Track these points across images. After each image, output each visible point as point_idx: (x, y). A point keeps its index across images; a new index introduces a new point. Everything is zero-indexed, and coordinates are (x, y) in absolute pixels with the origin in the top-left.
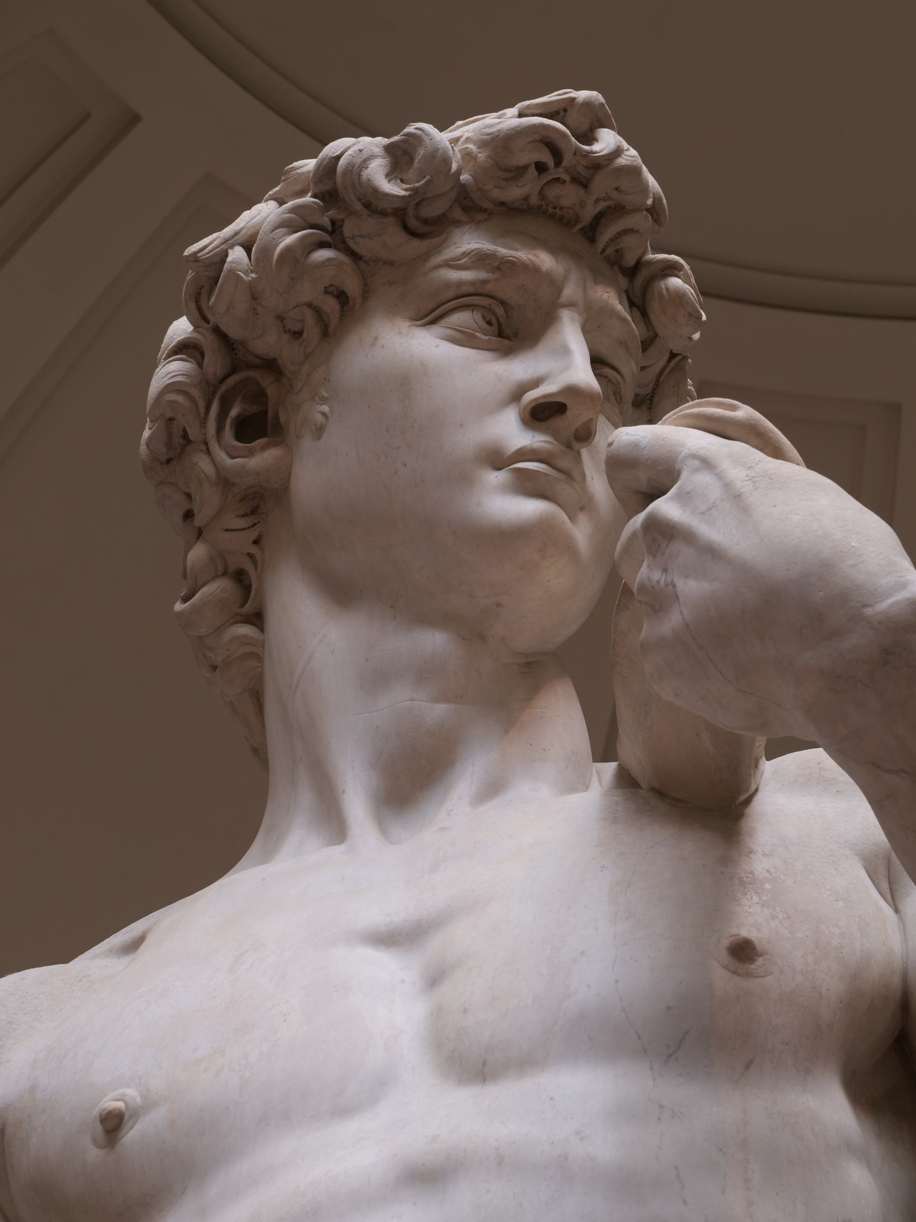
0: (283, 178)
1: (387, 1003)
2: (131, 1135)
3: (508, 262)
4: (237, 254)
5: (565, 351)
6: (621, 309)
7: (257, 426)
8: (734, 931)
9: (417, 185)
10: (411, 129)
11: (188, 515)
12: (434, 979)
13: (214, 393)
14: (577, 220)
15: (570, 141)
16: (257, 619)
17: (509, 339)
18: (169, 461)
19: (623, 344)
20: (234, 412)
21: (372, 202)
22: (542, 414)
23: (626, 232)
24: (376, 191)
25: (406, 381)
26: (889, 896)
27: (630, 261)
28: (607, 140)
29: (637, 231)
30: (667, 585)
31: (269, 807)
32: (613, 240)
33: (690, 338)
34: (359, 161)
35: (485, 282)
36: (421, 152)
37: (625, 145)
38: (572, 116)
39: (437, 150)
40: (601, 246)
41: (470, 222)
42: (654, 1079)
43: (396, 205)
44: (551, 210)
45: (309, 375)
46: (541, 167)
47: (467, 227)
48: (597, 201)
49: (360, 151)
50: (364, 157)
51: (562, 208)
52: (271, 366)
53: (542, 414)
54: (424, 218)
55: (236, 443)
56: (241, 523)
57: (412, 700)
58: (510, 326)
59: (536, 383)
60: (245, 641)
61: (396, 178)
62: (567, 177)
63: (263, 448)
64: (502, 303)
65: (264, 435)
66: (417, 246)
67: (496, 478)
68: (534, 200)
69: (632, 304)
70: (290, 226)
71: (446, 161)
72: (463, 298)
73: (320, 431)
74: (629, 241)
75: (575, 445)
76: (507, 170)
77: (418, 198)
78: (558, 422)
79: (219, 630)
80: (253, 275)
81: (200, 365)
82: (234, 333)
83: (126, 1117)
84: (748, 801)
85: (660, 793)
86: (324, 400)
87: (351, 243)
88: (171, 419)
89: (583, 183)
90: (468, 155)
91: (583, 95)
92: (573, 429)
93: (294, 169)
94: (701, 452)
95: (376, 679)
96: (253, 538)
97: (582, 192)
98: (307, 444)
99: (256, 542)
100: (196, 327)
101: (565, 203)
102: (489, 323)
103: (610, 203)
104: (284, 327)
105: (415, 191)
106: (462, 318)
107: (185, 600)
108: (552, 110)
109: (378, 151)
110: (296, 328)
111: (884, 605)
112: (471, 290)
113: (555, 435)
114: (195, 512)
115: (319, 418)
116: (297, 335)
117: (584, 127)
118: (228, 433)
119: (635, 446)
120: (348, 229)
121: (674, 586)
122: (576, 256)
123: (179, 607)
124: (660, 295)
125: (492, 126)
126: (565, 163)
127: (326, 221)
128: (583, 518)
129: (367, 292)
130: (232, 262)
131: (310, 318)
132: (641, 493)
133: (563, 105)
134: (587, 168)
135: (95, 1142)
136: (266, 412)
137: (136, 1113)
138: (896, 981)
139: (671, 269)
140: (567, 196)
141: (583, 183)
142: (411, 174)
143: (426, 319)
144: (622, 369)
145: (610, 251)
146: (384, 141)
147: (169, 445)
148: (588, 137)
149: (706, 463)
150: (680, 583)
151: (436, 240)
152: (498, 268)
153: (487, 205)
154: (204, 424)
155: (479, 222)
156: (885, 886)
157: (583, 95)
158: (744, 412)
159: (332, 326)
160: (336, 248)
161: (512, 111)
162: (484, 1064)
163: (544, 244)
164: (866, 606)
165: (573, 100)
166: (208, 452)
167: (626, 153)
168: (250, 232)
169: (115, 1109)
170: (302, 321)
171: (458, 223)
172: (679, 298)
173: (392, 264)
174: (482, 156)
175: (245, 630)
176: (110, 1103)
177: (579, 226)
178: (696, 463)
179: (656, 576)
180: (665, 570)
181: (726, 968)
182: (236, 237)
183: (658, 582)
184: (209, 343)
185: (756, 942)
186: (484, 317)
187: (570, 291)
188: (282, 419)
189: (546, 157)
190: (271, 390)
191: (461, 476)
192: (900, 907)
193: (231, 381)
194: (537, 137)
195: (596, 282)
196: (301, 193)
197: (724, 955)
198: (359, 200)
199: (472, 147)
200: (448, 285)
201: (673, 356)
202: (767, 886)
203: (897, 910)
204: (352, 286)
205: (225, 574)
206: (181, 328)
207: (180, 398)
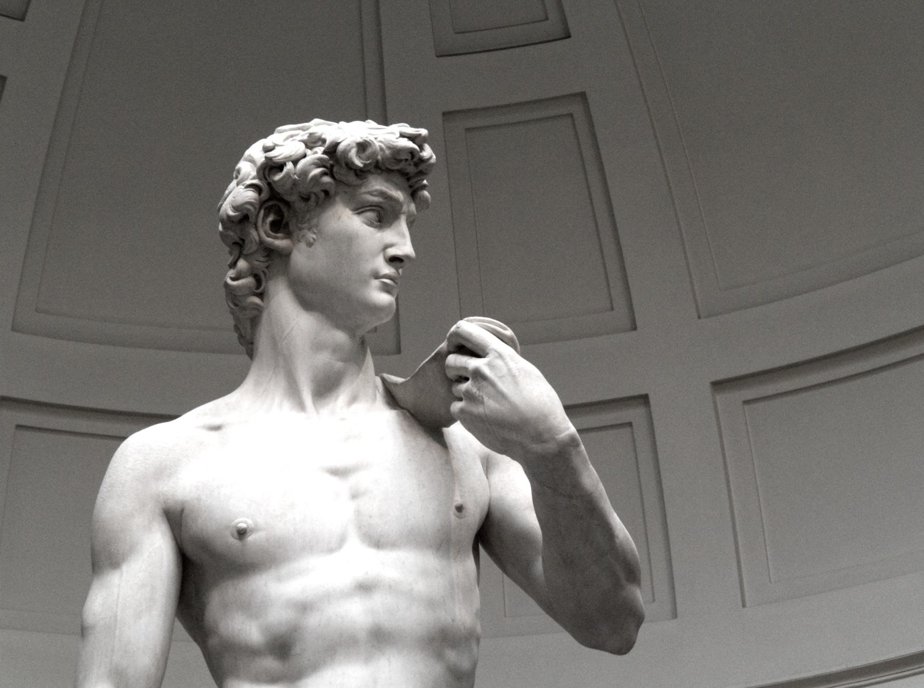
2: (251, 538)
5: (403, 236)
7: (278, 226)
12: (354, 496)
21: (350, 166)
24: (353, 163)
25: (349, 239)
36: (369, 151)
38: (417, 140)
46: (406, 160)
47: (375, 176)
52: (288, 204)
53: (394, 260)
56: (262, 259)
58: (383, 215)
63: (282, 239)
66: (359, 182)
67: (376, 283)
70: (318, 166)
72: (372, 207)
73: (310, 245)
77: (365, 165)
78: (398, 264)
81: (260, 194)
85: (412, 415)
90: (381, 149)
94: (499, 350)
95: (318, 347)
98: (303, 245)
99: (267, 268)
106: (371, 215)
107: (233, 279)
109: (354, 145)
115: (312, 240)
118: (267, 227)
119: (471, 335)
120: (335, 169)
127: (329, 165)
129: (336, 194)
135: (233, 536)
140: (411, 169)
142: (363, 155)
148: (422, 148)
149: (500, 356)
150: (486, 399)
154: (257, 216)
158: (509, 332)
165: (420, 135)
166: (256, 229)
171: (372, 173)
172: (425, 200)
173: (348, 185)
174: (387, 152)
175: (257, 300)
179: (474, 390)
180: (479, 389)
187: (405, 208)
189: (409, 157)
190: (286, 214)
191: (365, 282)
193: (270, 203)
197: (453, 509)
200: (368, 202)
204: (332, 192)
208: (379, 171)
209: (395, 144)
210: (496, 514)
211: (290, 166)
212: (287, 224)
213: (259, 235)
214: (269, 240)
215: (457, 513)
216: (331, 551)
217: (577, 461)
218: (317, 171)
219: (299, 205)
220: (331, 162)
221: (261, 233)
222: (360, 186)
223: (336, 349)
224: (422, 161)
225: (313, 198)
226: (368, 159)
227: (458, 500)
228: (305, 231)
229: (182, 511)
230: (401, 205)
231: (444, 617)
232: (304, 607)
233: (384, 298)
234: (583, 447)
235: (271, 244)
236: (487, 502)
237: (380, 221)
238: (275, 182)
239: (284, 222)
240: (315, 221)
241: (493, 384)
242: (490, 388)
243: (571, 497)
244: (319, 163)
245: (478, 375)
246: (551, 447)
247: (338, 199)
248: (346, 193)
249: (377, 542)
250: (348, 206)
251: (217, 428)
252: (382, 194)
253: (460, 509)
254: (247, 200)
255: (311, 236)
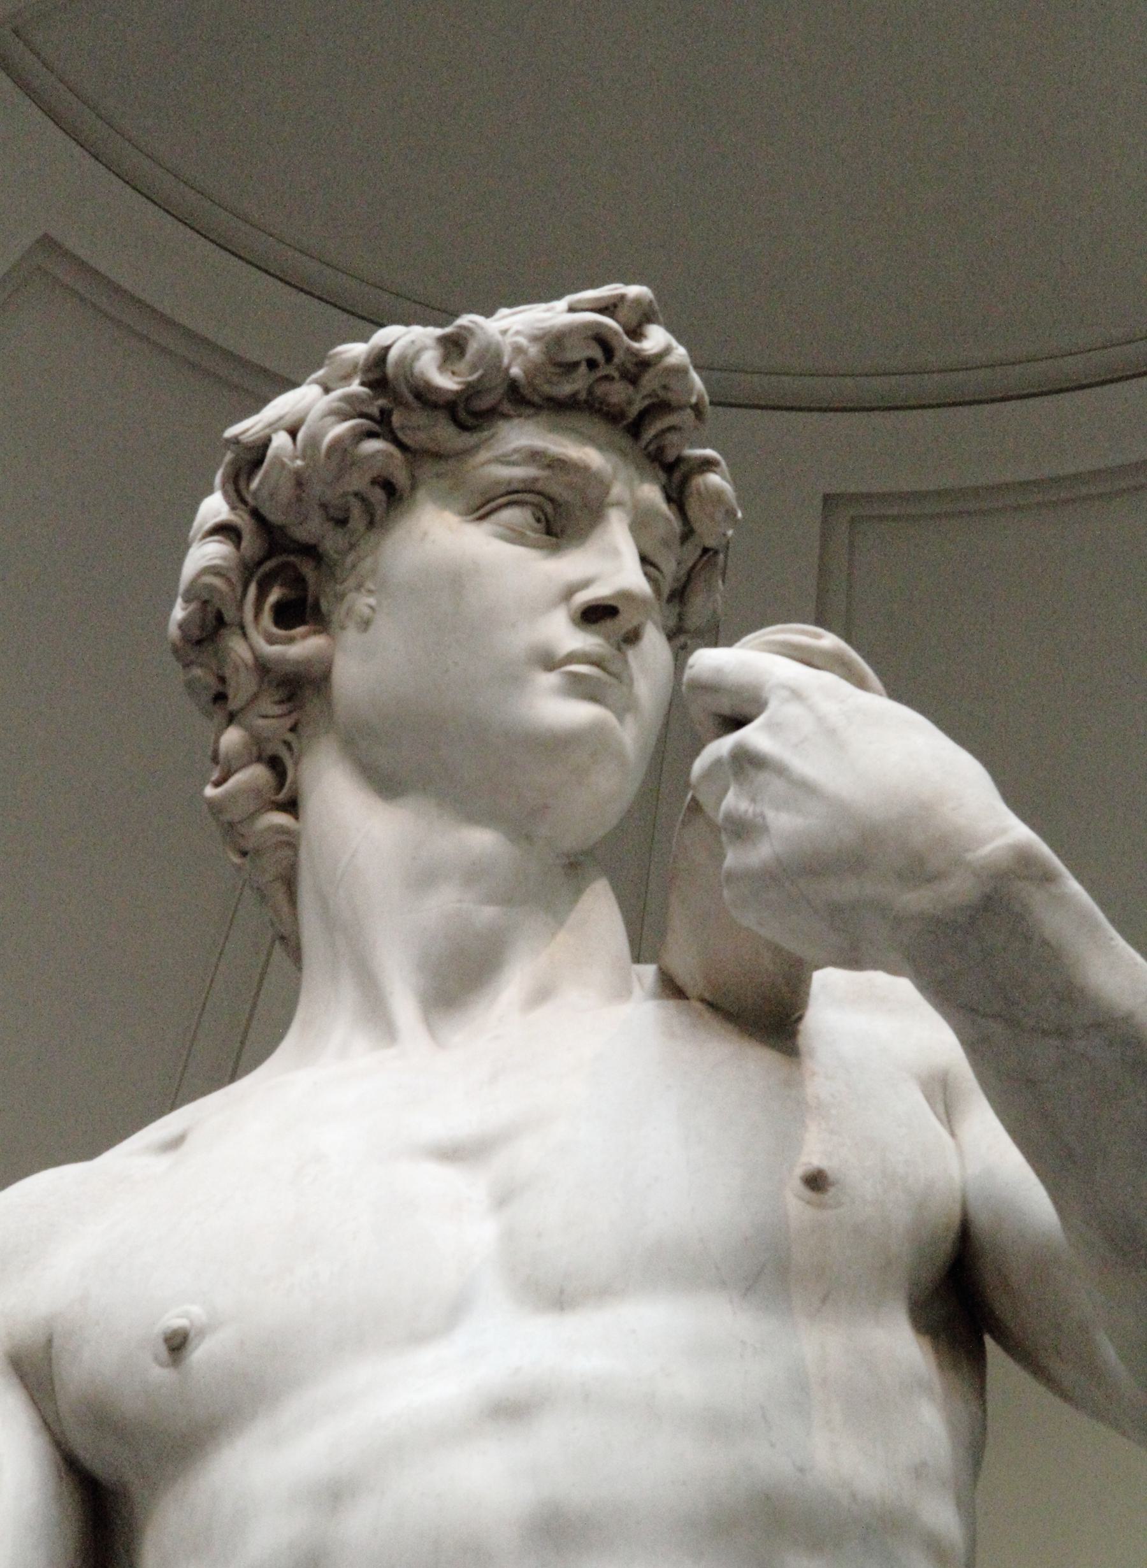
0: (327, 362)
1: (460, 1226)
2: (199, 1354)
3: (559, 460)
4: (281, 440)
5: (616, 553)
6: (664, 507)
7: (297, 612)
8: (804, 1159)
9: (470, 379)
10: (465, 320)
11: (220, 698)
12: (503, 1199)
13: (252, 575)
14: (622, 415)
15: (622, 340)
16: (291, 806)
17: (556, 536)
18: (199, 642)
19: (665, 543)
20: (274, 596)
21: (425, 397)
22: (594, 615)
23: (671, 429)
25: (456, 579)
26: (944, 1117)
27: (671, 456)
28: (656, 338)
29: (680, 429)
30: (755, 815)
31: (303, 999)
32: (656, 437)
33: (725, 535)
34: (411, 352)
35: (536, 480)
36: (473, 347)
37: (674, 343)
38: (623, 312)
39: (489, 344)
40: (643, 443)
41: (520, 416)
42: (735, 1313)
43: (451, 397)
44: (597, 405)
45: (354, 566)
46: (592, 364)
47: (516, 421)
48: (644, 398)
49: (413, 342)
50: (416, 348)
51: (608, 405)
52: (311, 551)
53: (594, 615)
54: (471, 412)
55: (275, 630)
56: (277, 710)
57: (460, 901)
59: (586, 584)
60: (281, 830)
61: (447, 369)
62: (616, 375)
63: (304, 637)
64: (552, 500)
65: (303, 622)
68: (583, 396)
69: (669, 499)
71: (498, 355)
73: (365, 624)
74: (672, 437)
75: (624, 646)
76: (559, 365)
77: (471, 391)
78: (609, 624)
79: (253, 816)
80: (299, 463)
82: (275, 517)
83: (192, 1334)
84: (800, 1018)
85: (713, 1006)
86: (370, 592)
87: (400, 435)
88: (205, 603)
89: (633, 380)
90: (518, 350)
91: (634, 291)
92: (624, 631)
93: (340, 353)
95: (424, 878)
96: (288, 726)
97: (631, 388)
98: (351, 636)
99: (293, 729)
100: (233, 508)
101: (614, 399)
102: (538, 520)
103: (655, 400)
104: (327, 513)
105: (469, 385)
107: (217, 784)
108: (603, 304)
109: (430, 342)
110: (340, 515)
111: (986, 850)
112: (521, 486)
113: (607, 638)
114: (231, 697)
115: (367, 611)
116: (342, 522)
117: (634, 323)
119: (719, 671)
120: (396, 419)
121: (764, 818)
122: (623, 453)
123: (210, 791)
124: (699, 494)
125: (543, 320)
126: (616, 360)
127: (374, 410)
128: (629, 719)
130: (277, 448)
131: (356, 511)
132: (720, 716)
133: (612, 301)
134: (636, 364)
135: (156, 1358)
136: (306, 596)
137: (202, 1333)
138: (957, 1209)
139: (708, 465)
140: (617, 392)
141: (633, 380)
142: (462, 366)
143: (477, 514)
144: (663, 567)
145: (652, 448)
146: (439, 332)
147: (202, 628)
148: (636, 333)
149: (796, 694)
151: (486, 434)
152: (549, 466)
153: (536, 399)
154: (240, 606)
155: (528, 417)
156: (941, 1109)
157: (634, 291)
158: (829, 641)
159: (378, 518)
160: (386, 439)
161: (562, 304)
162: (562, 1292)
163: (591, 440)
164: (967, 850)
165: (622, 297)
166: (245, 635)
167: (675, 351)
168: (295, 418)
169: (180, 1328)
170: (348, 510)
171: (506, 417)
172: (717, 497)
173: (438, 456)
174: (533, 350)
175: (280, 819)
176: (174, 1320)
177: (625, 423)
178: (785, 693)
180: (753, 800)
181: (800, 1198)
182: (282, 422)
183: (746, 811)
184: (242, 520)
185: (829, 1173)
186: (534, 514)
187: (617, 490)
188: (324, 606)
189: (597, 353)
191: (512, 678)
192: (957, 1132)
194: (590, 333)
195: (642, 482)
196: (346, 378)
198: (411, 392)
199: (523, 341)
200: (498, 483)
201: (705, 550)
202: (834, 1112)
203: (953, 1134)
204: (401, 477)
205: (259, 759)
206: (215, 507)
207: (217, 582)
208: (531, 411)
209: (546, 324)
210: (982, 1220)
211: (281, 440)
212: (317, 606)
213: (252, 648)
214: (276, 649)
215: (808, 1193)
216: (419, 1337)
217: (1053, 922)
218: (341, 428)
219: (332, 541)
220: (381, 402)
221: (258, 641)
222: (476, 448)
223: (474, 874)
224: (645, 363)
225: (356, 511)
226: (474, 368)
227: (813, 1157)
228: (351, 596)
229: (50, 1341)
230: (605, 487)
231: (769, 1459)
232: (335, 1494)
233: (578, 713)
234: (1074, 886)
235: (282, 660)
236: (958, 1195)
237: (549, 532)
238: (255, 494)
239: (310, 600)
240: (369, 560)
241: (780, 770)
242: (777, 785)
243: (1063, 1033)
244: (350, 409)
245: (746, 762)
246: (959, 889)
247: (421, 494)
248: (439, 476)
249: (555, 1294)
250: (446, 506)
251: (175, 1143)
252: (534, 456)
253: (816, 1181)
254: (204, 563)
255: (363, 602)
